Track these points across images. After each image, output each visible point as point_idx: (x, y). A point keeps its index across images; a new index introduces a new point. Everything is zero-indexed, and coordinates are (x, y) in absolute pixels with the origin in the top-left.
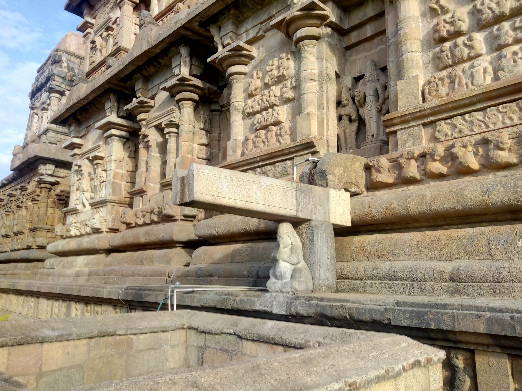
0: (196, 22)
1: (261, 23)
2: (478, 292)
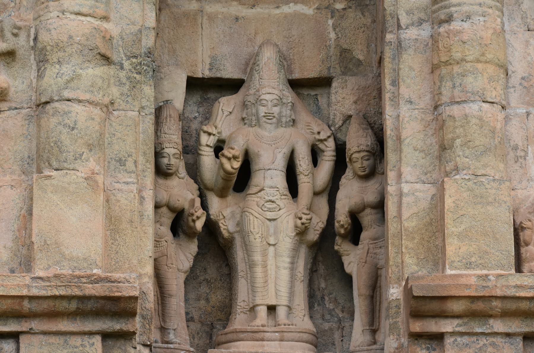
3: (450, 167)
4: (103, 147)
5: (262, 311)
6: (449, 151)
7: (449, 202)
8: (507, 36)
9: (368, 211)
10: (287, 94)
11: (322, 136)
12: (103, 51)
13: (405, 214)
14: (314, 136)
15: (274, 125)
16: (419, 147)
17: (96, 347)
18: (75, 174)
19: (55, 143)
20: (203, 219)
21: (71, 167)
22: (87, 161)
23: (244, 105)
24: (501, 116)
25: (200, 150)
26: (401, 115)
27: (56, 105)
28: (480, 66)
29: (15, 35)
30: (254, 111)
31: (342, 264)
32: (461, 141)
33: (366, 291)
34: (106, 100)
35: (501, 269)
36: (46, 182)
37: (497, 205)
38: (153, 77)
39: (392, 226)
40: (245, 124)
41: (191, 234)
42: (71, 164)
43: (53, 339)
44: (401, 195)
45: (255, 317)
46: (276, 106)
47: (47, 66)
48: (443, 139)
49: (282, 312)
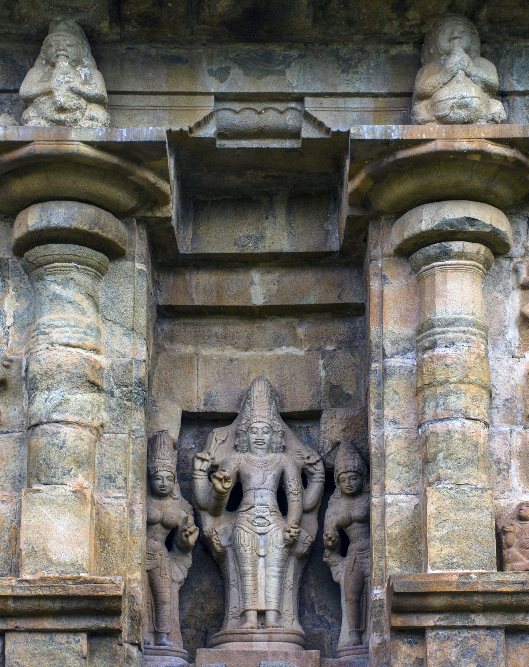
4: (93, 465)
5: (252, 617)
6: (432, 464)
10: (278, 423)
11: (311, 461)
14: (304, 461)
15: (264, 451)
16: (402, 462)
17: (82, 644)
18: (63, 488)
19: (44, 460)
21: (60, 481)
22: (75, 476)
23: (237, 434)
25: (194, 474)
26: (385, 434)
30: (245, 438)
31: (330, 574)
32: (444, 454)
35: (483, 569)
36: (35, 495)
37: (479, 511)
40: (237, 451)
42: (59, 479)
45: (246, 621)
46: (266, 433)
48: (426, 454)
49: (271, 617)
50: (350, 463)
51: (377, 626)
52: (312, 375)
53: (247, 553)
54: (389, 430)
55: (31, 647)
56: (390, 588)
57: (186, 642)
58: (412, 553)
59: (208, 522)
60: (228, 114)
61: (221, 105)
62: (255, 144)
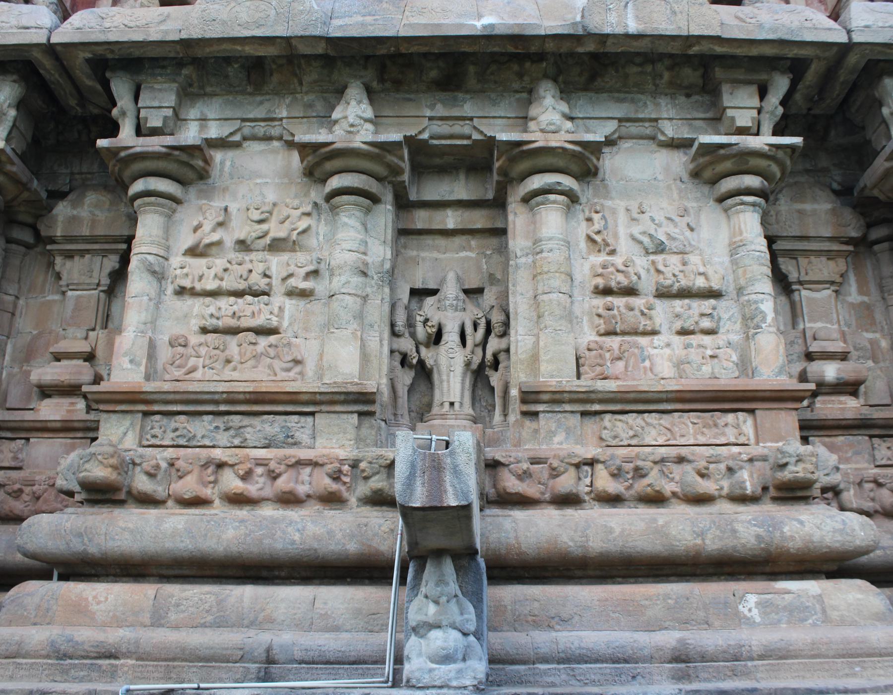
0: (91, 52)
1: (244, 120)
2: (714, 674)
3: (542, 326)
5: (447, 405)
7: (542, 344)
8: (572, 261)
9: (502, 353)
11: (479, 316)
12: (362, 269)
13: (519, 352)
20: (417, 358)
23: (439, 301)
24: (569, 300)
27: (338, 296)
28: (557, 274)
29: (319, 263)
33: (501, 394)
34: (364, 294)
38: (389, 284)
39: (513, 357)
41: (411, 366)
43: (332, 415)
44: (517, 341)
45: (443, 408)
47: (334, 277)
48: (539, 312)
49: (457, 405)
50: (499, 318)
51: (513, 410)
52: (479, 268)
53: (444, 369)
54: (519, 298)
55: (328, 421)
56: (520, 389)
57: (411, 419)
58: (532, 369)
59: (423, 350)
60: (435, 127)
61: (431, 122)
62: (448, 142)
